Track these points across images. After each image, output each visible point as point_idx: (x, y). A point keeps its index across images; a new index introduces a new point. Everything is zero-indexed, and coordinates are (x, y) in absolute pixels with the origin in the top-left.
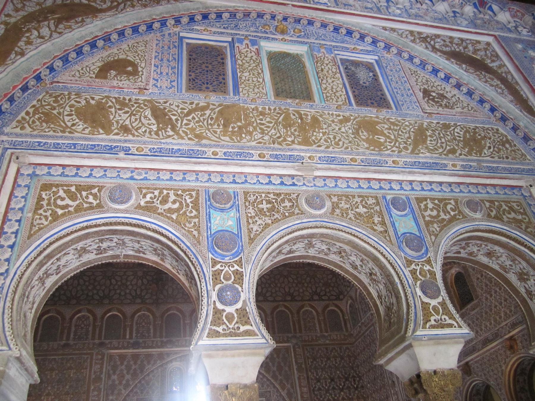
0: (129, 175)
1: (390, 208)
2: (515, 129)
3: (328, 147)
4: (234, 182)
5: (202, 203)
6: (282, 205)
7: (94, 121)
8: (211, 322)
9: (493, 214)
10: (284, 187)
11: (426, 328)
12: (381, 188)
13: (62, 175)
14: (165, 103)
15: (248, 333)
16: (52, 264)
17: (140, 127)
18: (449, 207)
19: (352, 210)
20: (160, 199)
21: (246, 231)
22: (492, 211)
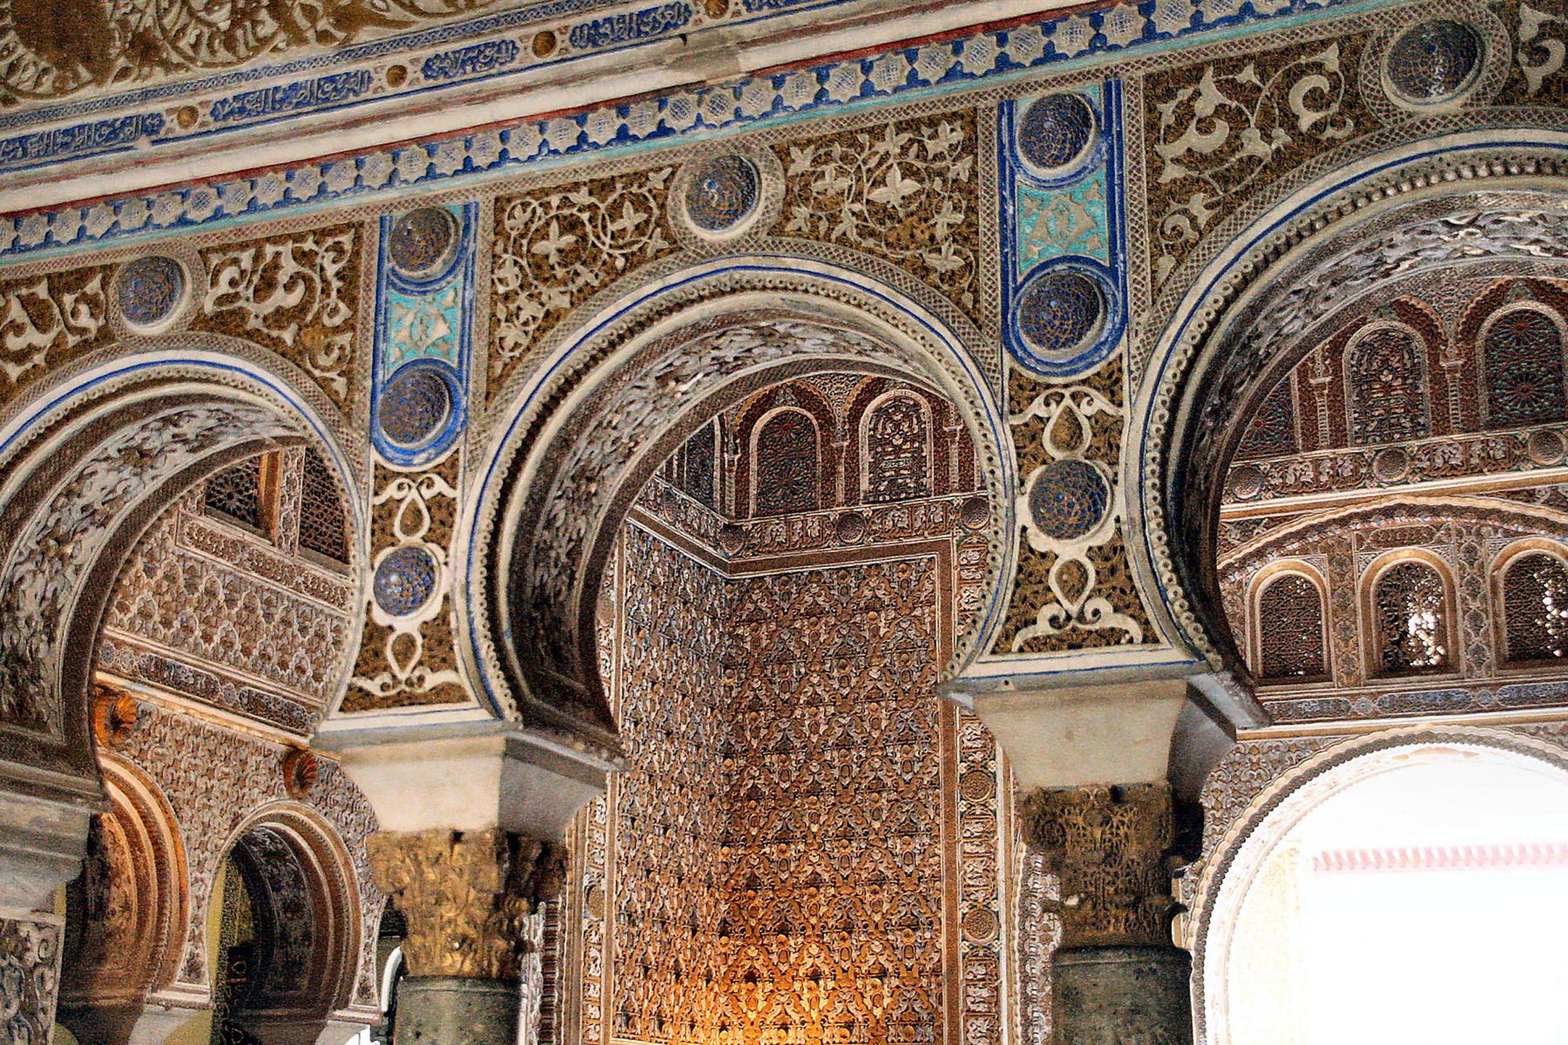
0: (174, 210)
1: (1015, 157)
4: (468, 167)
5: (368, 273)
6: (611, 227)
7: (61, 41)
8: (357, 666)
10: (629, 149)
11: (1010, 651)
15: (446, 694)
16: (53, 509)
17: (183, 29)
19: (858, 197)
20: (256, 279)
21: (485, 353)
22: (1539, 54)
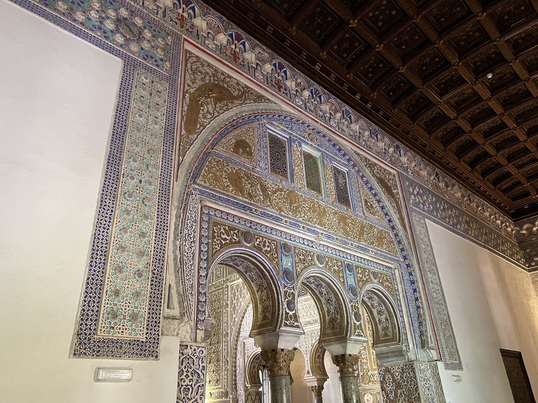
2: (396, 235)
3: (328, 229)
7: (236, 187)
9: (381, 281)
10: (308, 247)
12: (343, 257)
13: (221, 217)
14: (266, 181)
18: (366, 273)
